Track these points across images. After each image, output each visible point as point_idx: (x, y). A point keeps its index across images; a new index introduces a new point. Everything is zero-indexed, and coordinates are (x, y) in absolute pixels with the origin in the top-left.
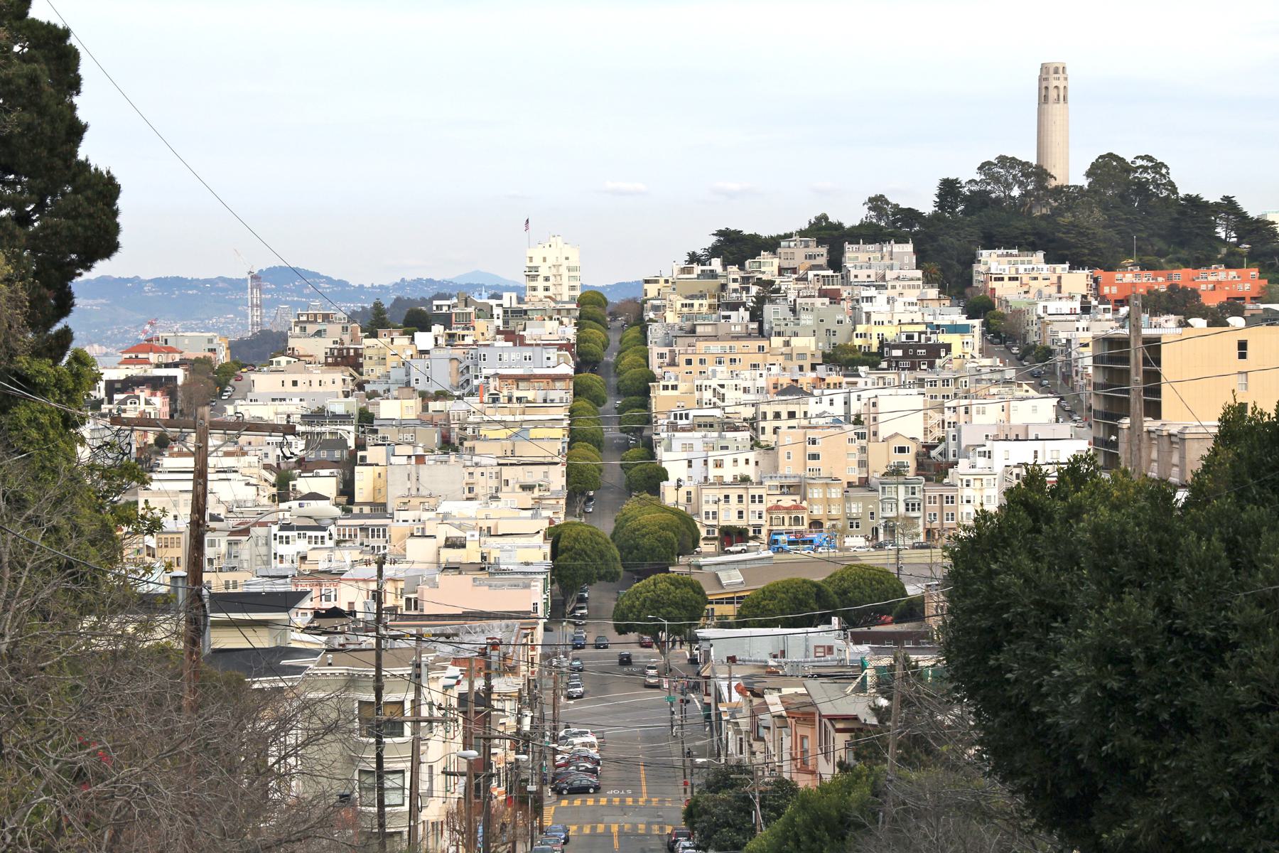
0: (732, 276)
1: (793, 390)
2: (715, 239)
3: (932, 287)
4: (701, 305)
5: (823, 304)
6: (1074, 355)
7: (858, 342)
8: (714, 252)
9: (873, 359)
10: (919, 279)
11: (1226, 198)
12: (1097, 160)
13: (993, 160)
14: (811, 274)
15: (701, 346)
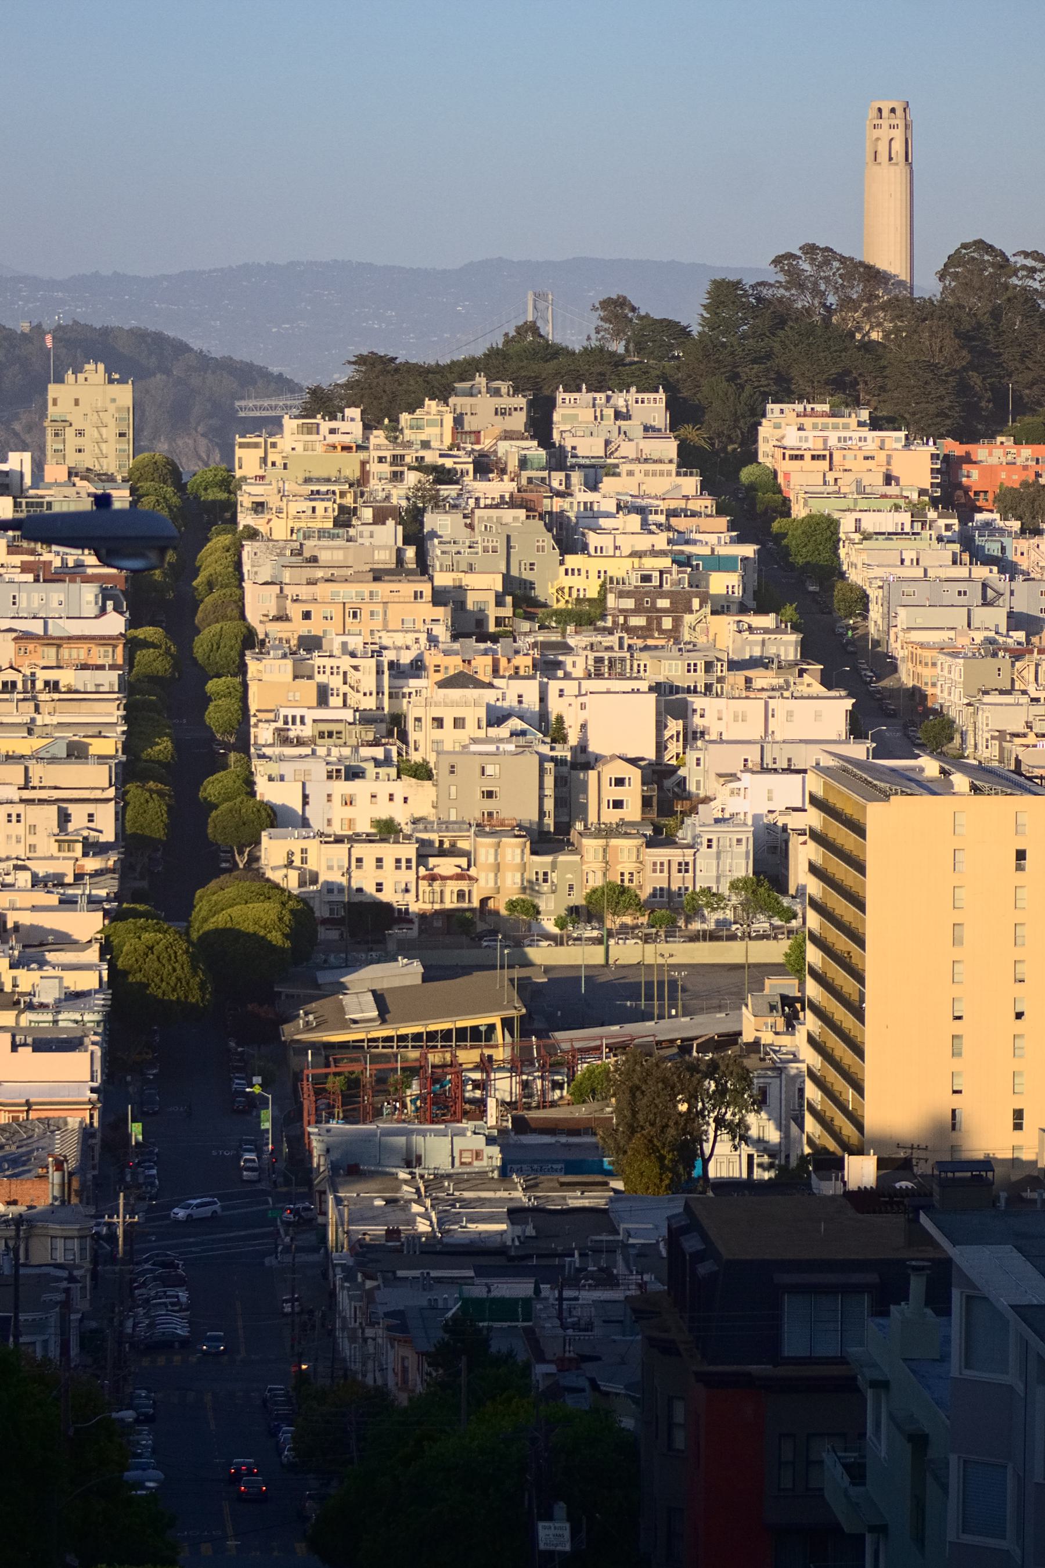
3: (691, 474)
5: (516, 519)
10: (671, 461)
12: (958, 251)
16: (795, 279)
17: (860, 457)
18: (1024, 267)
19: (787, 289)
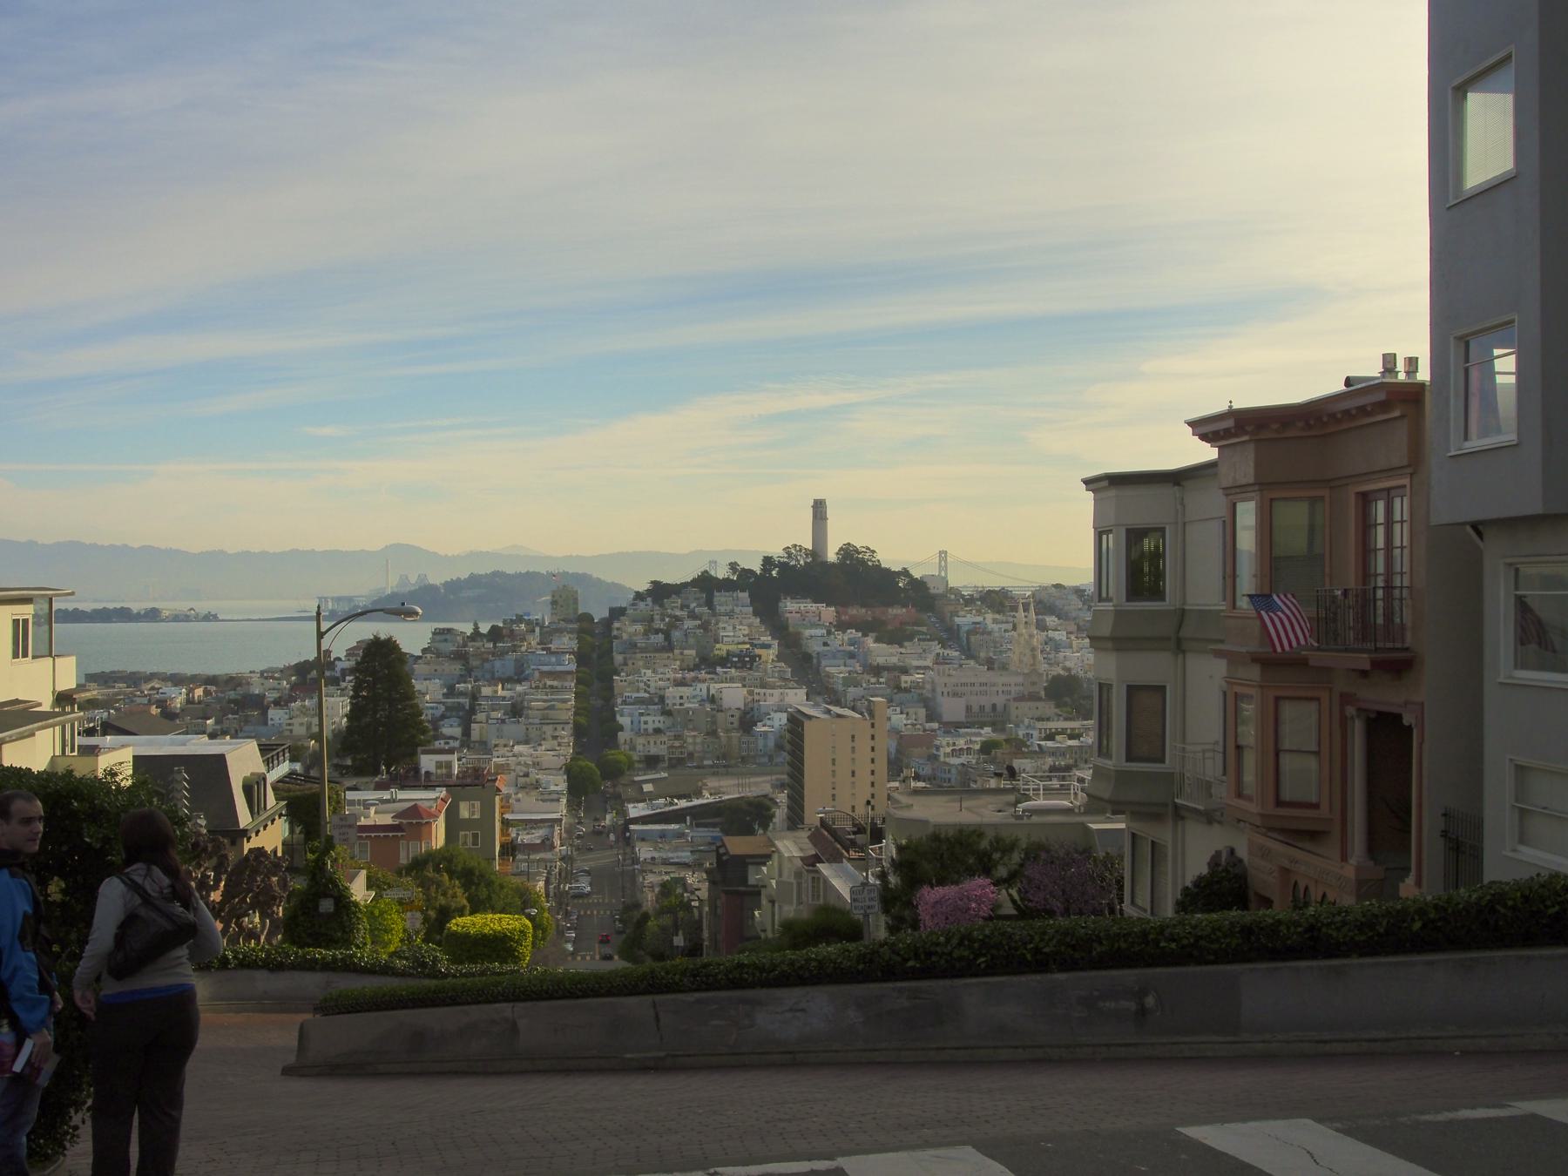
7: (716, 652)
9: (724, 661)
11: (905, 569)
16: (790, 555)
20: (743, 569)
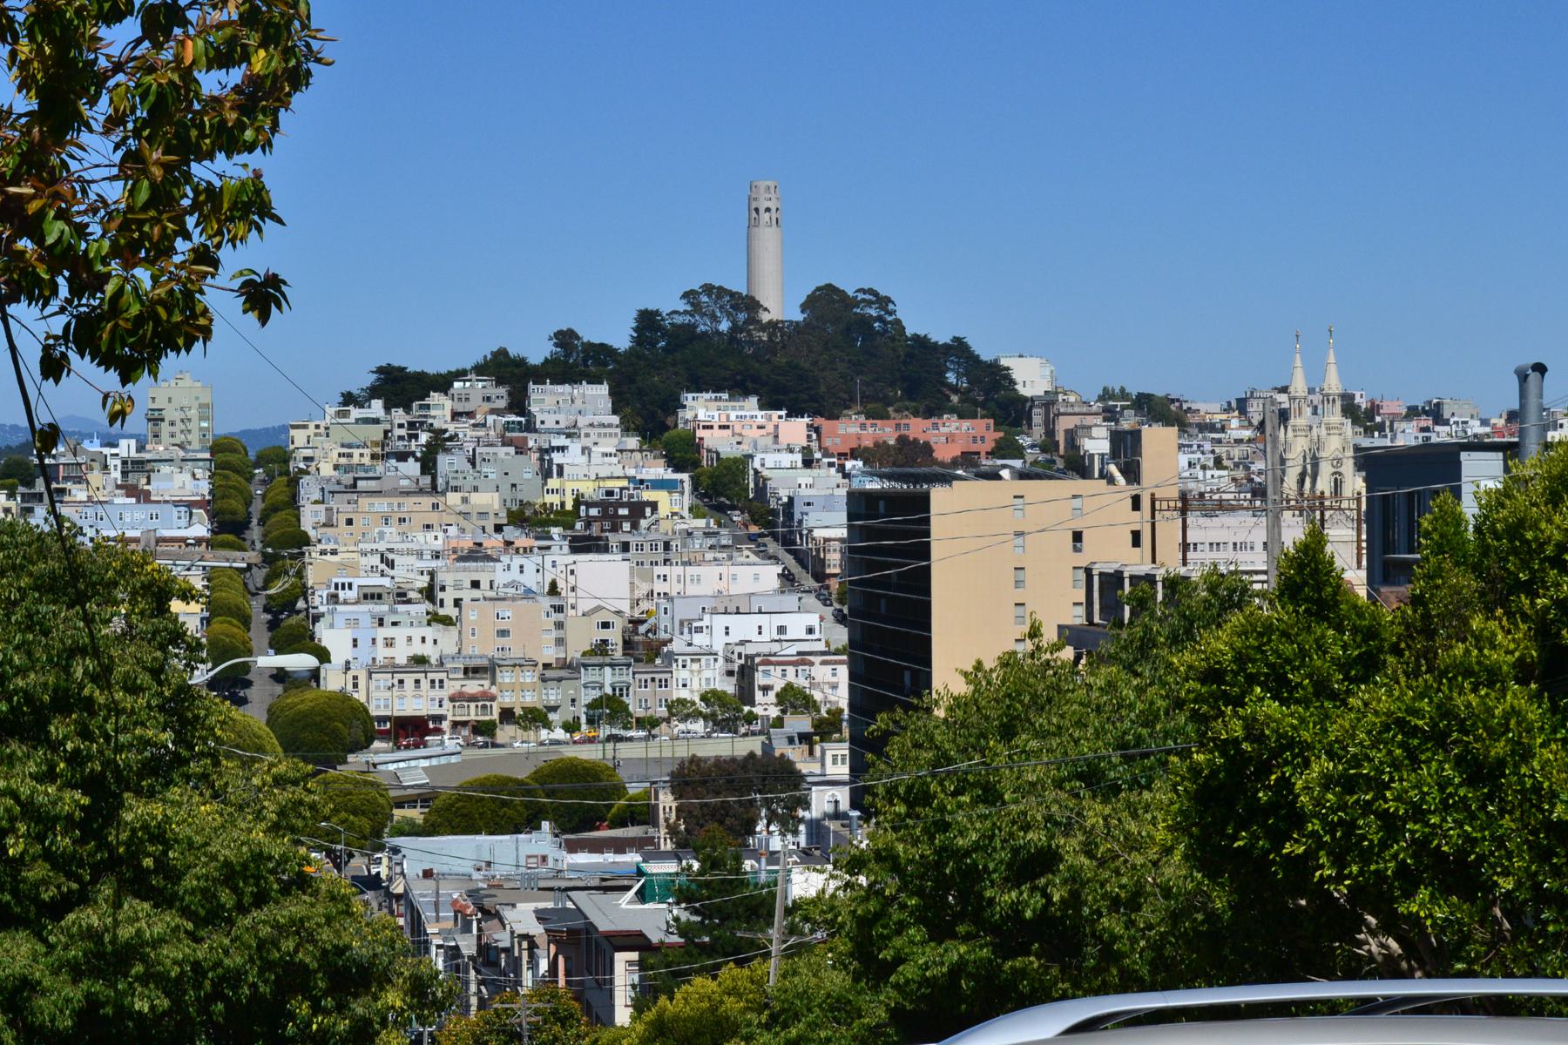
0: (397, 421)
1: (476, 554)
2: (375, 376)
4: (362, 455)
5: (507, 454)
6: (797, 516)
8: (374, 392)
11: (956, 339)
12: (814, 292)
13: (696, 288)
14: (491, 419)
15: (364, 502)
16: (697, 307)
17: (755, 427)
18: (863, 300)
19: (692, 316)
20: (591, 345)
